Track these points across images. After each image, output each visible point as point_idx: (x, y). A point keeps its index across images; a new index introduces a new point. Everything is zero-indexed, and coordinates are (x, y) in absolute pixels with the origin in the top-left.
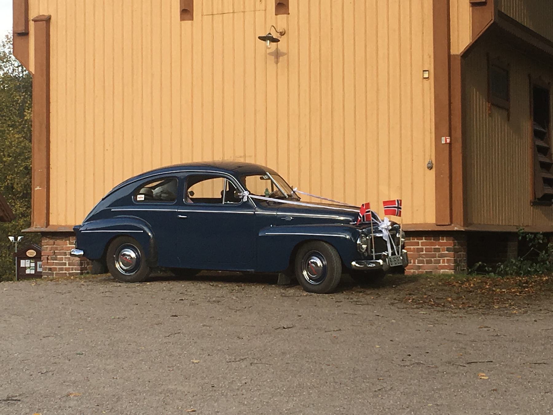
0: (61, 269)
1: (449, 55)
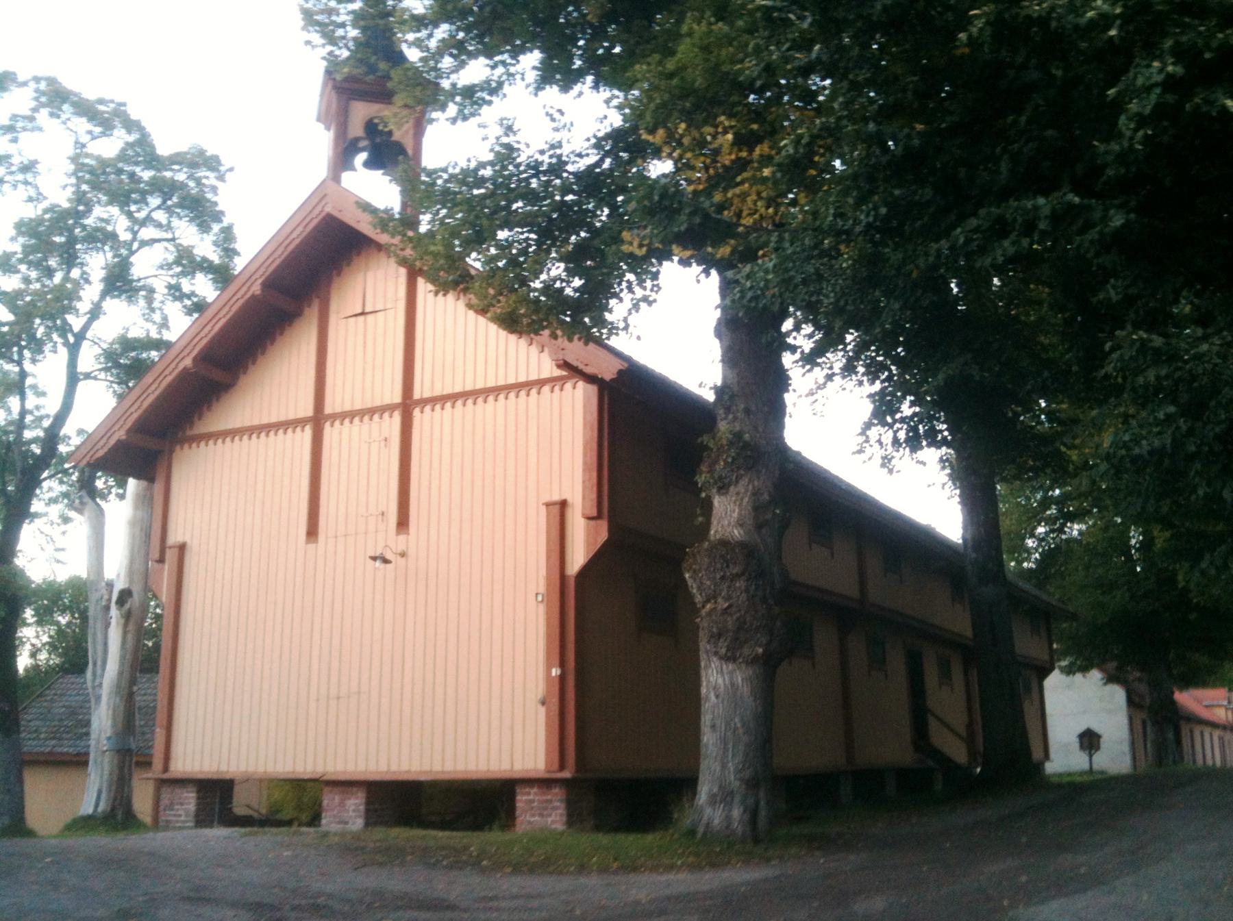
0: (177, 822)
1: (563, 577)
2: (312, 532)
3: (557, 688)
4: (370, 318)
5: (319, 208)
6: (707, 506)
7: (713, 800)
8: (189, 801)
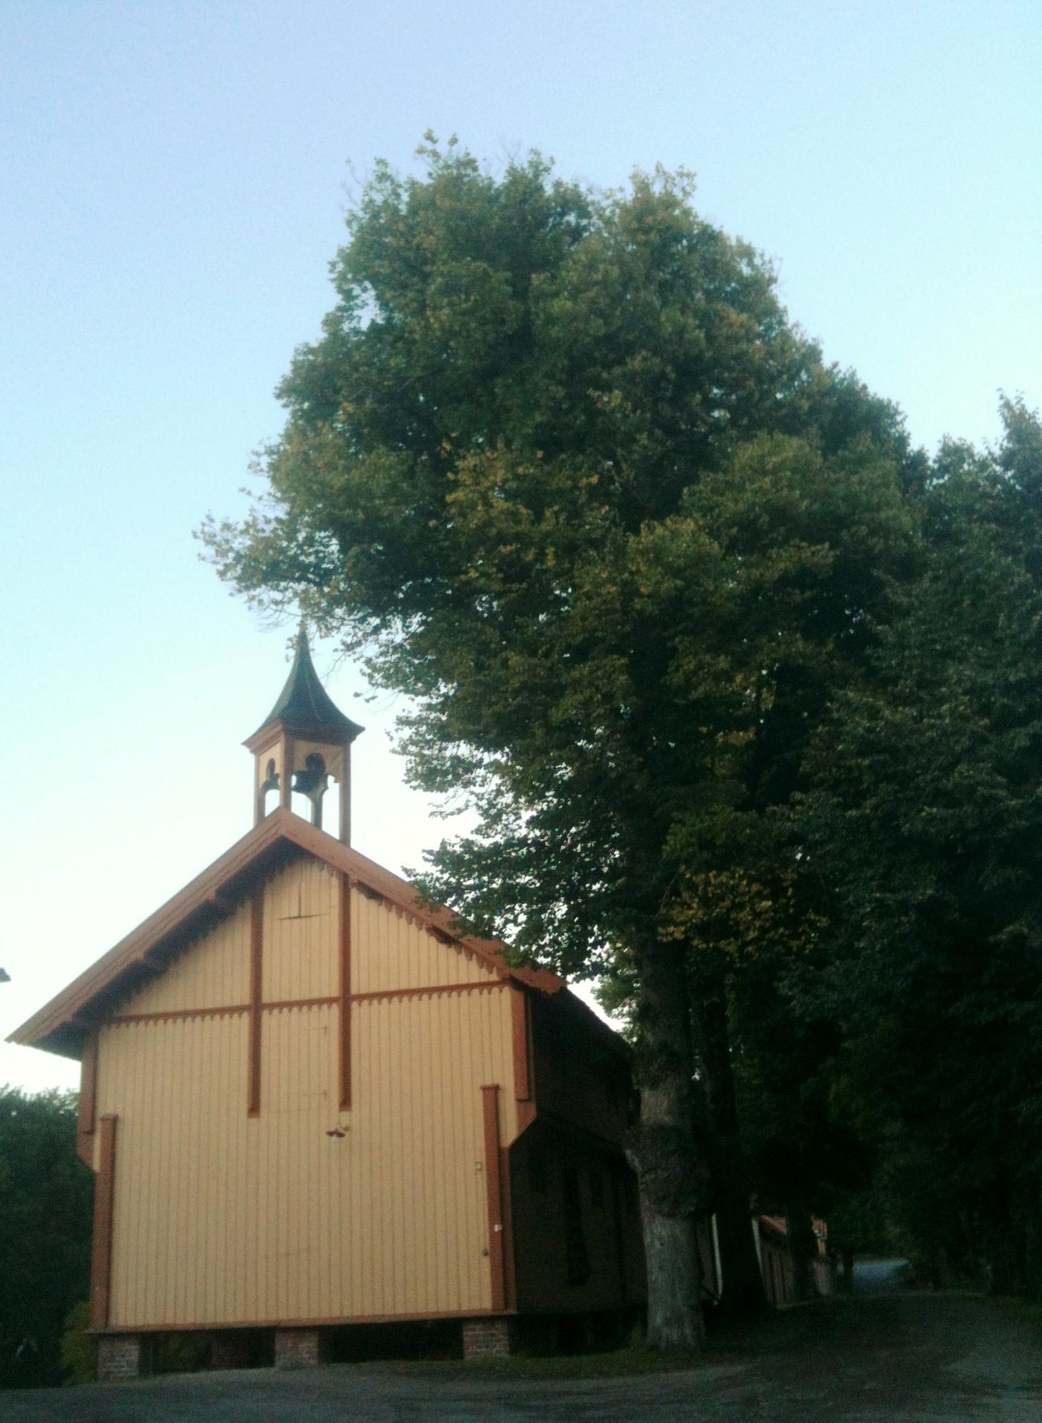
2: (254, 1109)
3: (498, 1239)
4: (304, 920)
5: (274, 830)
6: (638, 1100)
7: (667, 1323)
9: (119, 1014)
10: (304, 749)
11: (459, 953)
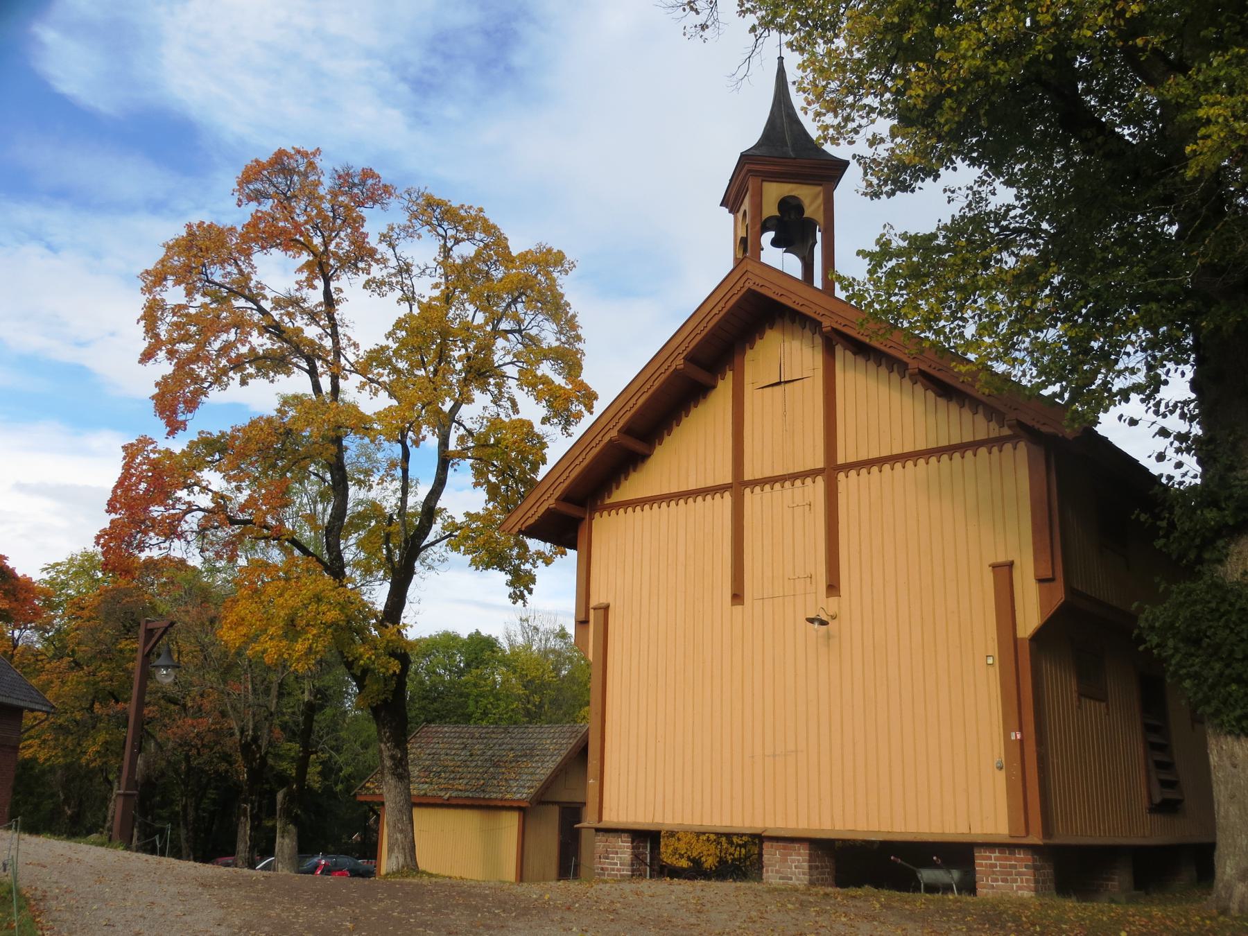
0: (613, 870)
1: (1015, 639)
2: (737, 597)
3: (1018, 750)
8: (623, 850)
9: (608, 501)
10: (774, 192)
11: (975, 413)
